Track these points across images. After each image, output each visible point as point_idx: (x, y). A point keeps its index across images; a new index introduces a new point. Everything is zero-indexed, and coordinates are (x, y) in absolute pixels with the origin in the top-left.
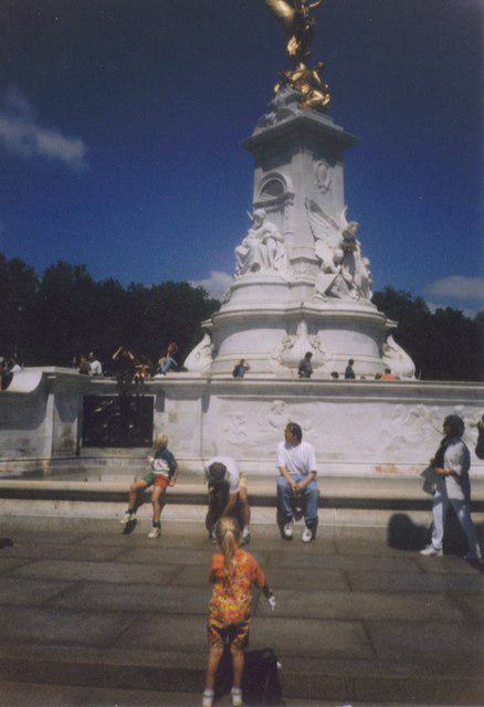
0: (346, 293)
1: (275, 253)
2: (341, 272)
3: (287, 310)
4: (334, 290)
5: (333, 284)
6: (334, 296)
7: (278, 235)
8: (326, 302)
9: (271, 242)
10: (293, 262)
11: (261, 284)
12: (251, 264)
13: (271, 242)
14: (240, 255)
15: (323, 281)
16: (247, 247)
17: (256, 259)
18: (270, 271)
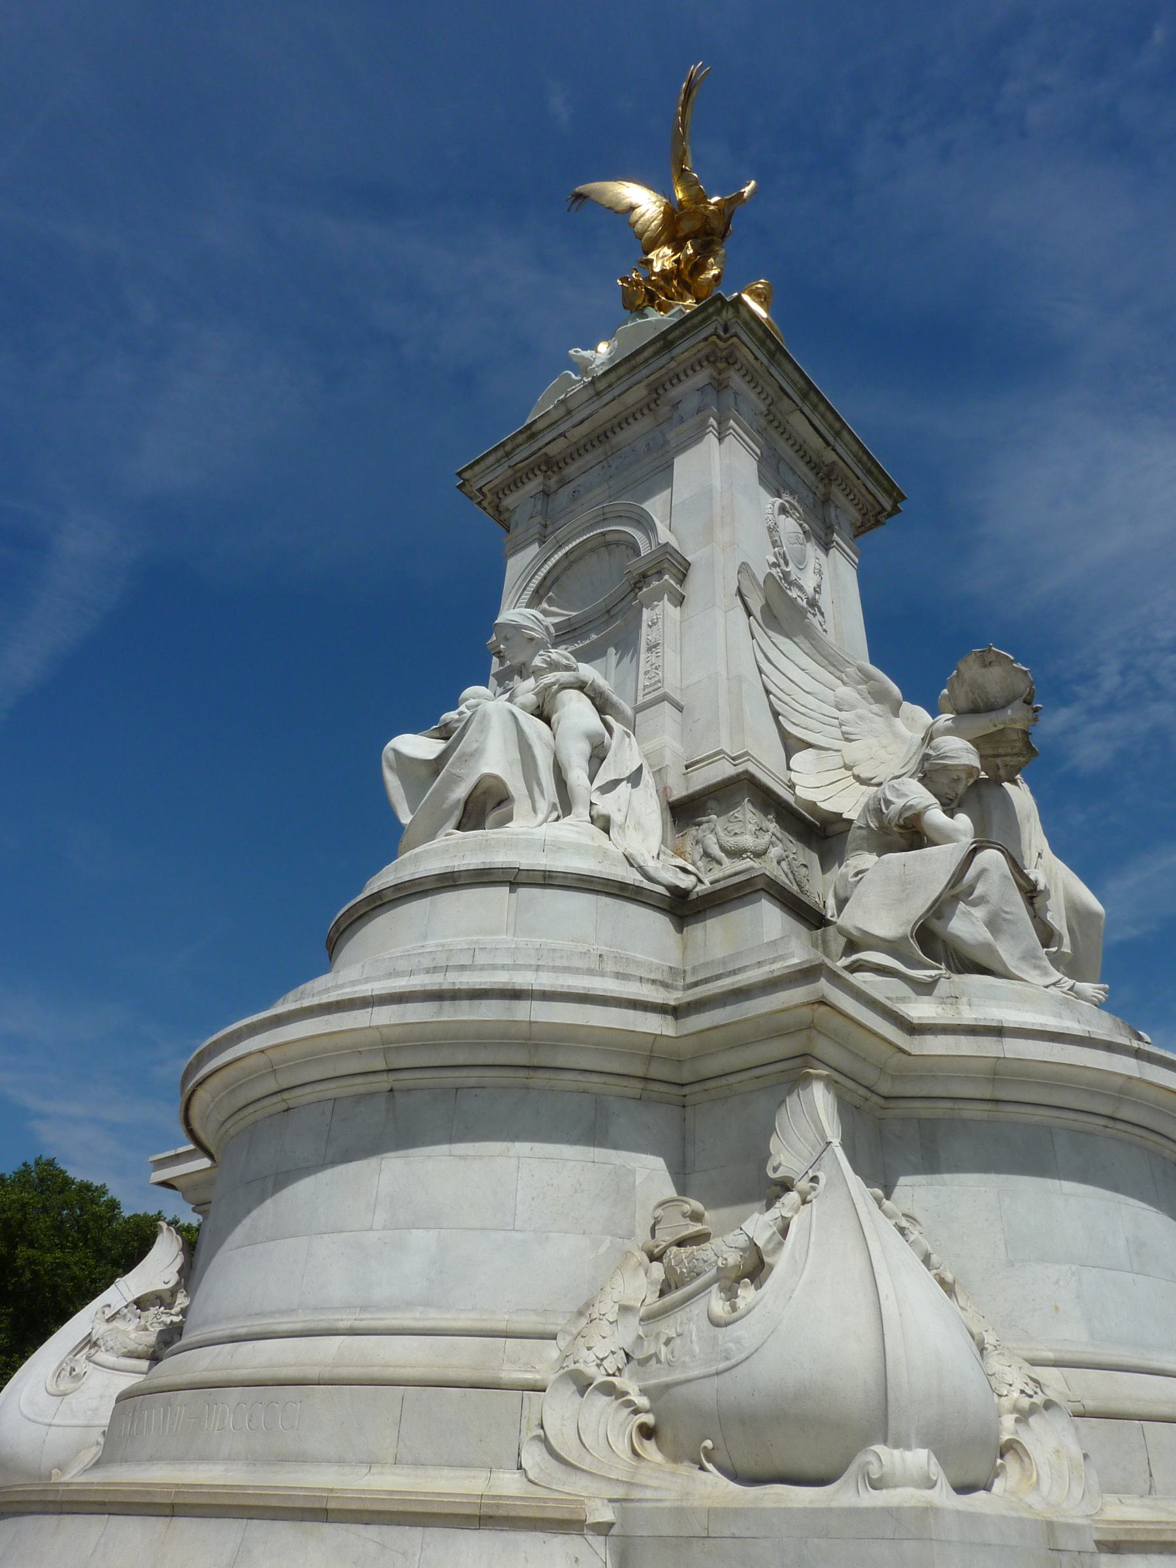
1: (598, 756)
4: (966, 926)
5: (957, 891)
6: (966, 962)
12: (461, 792)
15: (880, 896)
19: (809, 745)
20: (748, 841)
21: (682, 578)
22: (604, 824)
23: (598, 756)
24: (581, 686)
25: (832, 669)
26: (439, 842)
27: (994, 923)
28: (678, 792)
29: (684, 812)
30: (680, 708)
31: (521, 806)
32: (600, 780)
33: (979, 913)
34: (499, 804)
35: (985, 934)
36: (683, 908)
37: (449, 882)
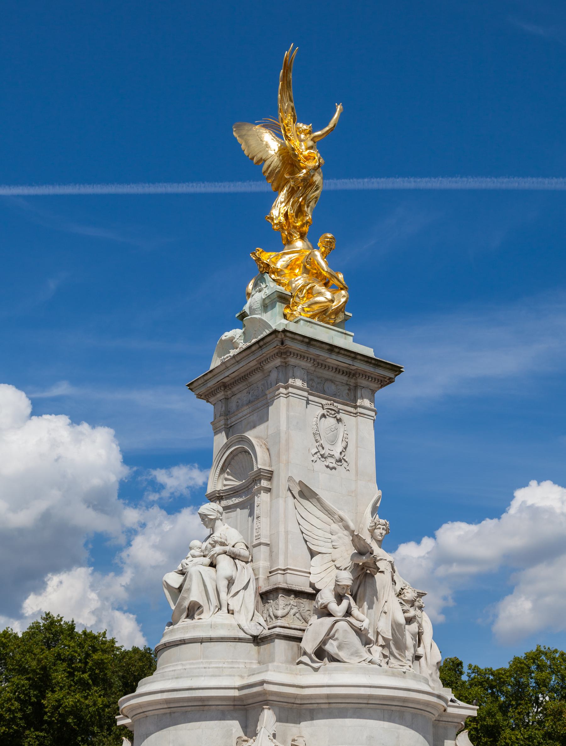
0: (356, 653)
1: (231, 582)
2: (348, 613)
3: (240, 688)
5: (329, 636)
6: (333, 659)
7: (241, 549)
8: (316, 670)
9: (225, 563)
10: (265, 597)
11: (201, 641)
12: (186, 604)
13: (225, 563)
14: (169, 587)
16: (182, 573)
17: (195, 594)
18: (222, 617)
19: (320, 553)
20: (280, 613)
21: (270, 479)
22: (230, 612)
23: (231, 582)
24: (225, 553)
25: (329, 516)
26: (180, 624)
27: (340, 647)
28: (264, 589)
29: (265, 597)
30: (267, 545)
31: (205, 608)
32: (232, 592)
33: (335, 643)
34: (199, 608)
35: (336, 651)
36: (257, 640)
37: (183, 642)
